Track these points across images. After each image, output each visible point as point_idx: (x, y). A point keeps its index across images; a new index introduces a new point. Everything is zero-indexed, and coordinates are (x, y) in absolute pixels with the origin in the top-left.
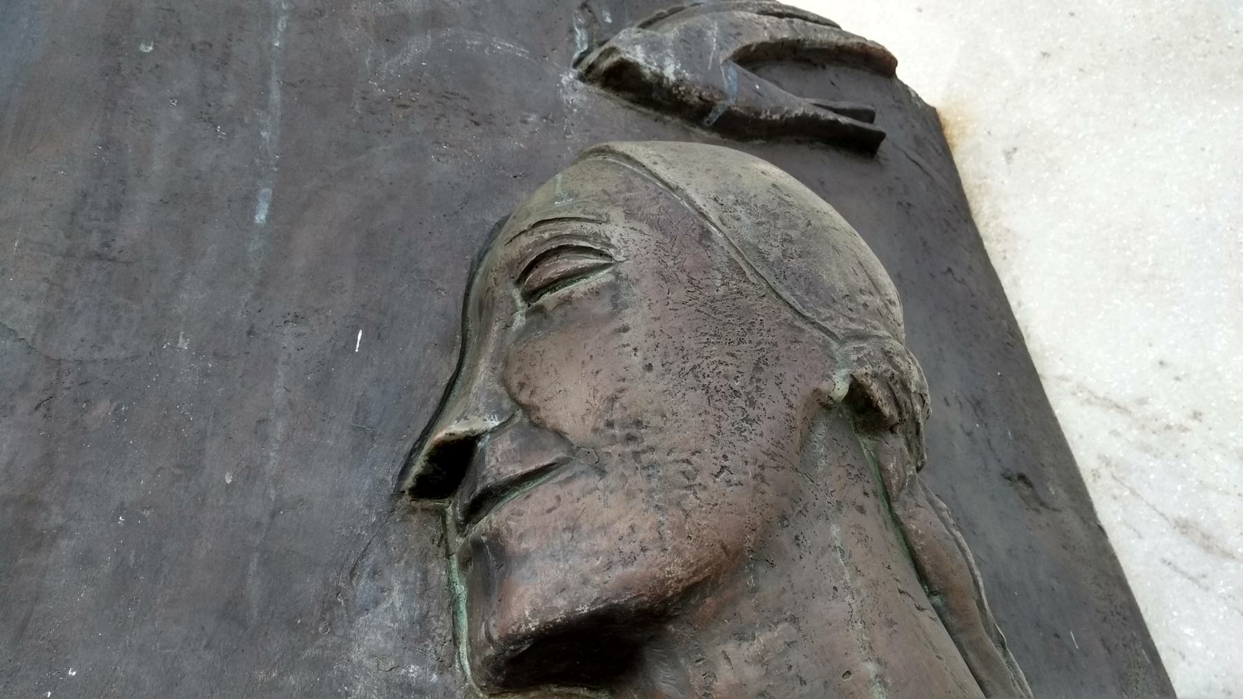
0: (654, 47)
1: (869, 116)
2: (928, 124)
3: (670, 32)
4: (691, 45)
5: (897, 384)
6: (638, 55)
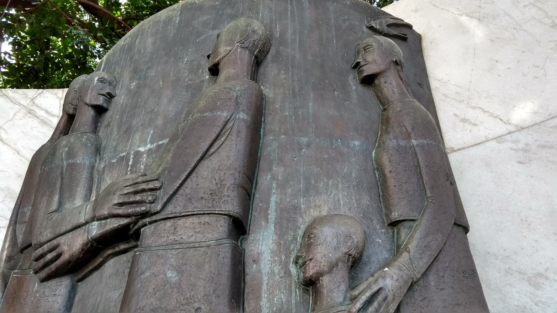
0: (376, 24)
1: (406, 35)
2: (419, 38)
3: (378, 22)
4: (381, 24)
5: (400, 61)
6: (374, 25)
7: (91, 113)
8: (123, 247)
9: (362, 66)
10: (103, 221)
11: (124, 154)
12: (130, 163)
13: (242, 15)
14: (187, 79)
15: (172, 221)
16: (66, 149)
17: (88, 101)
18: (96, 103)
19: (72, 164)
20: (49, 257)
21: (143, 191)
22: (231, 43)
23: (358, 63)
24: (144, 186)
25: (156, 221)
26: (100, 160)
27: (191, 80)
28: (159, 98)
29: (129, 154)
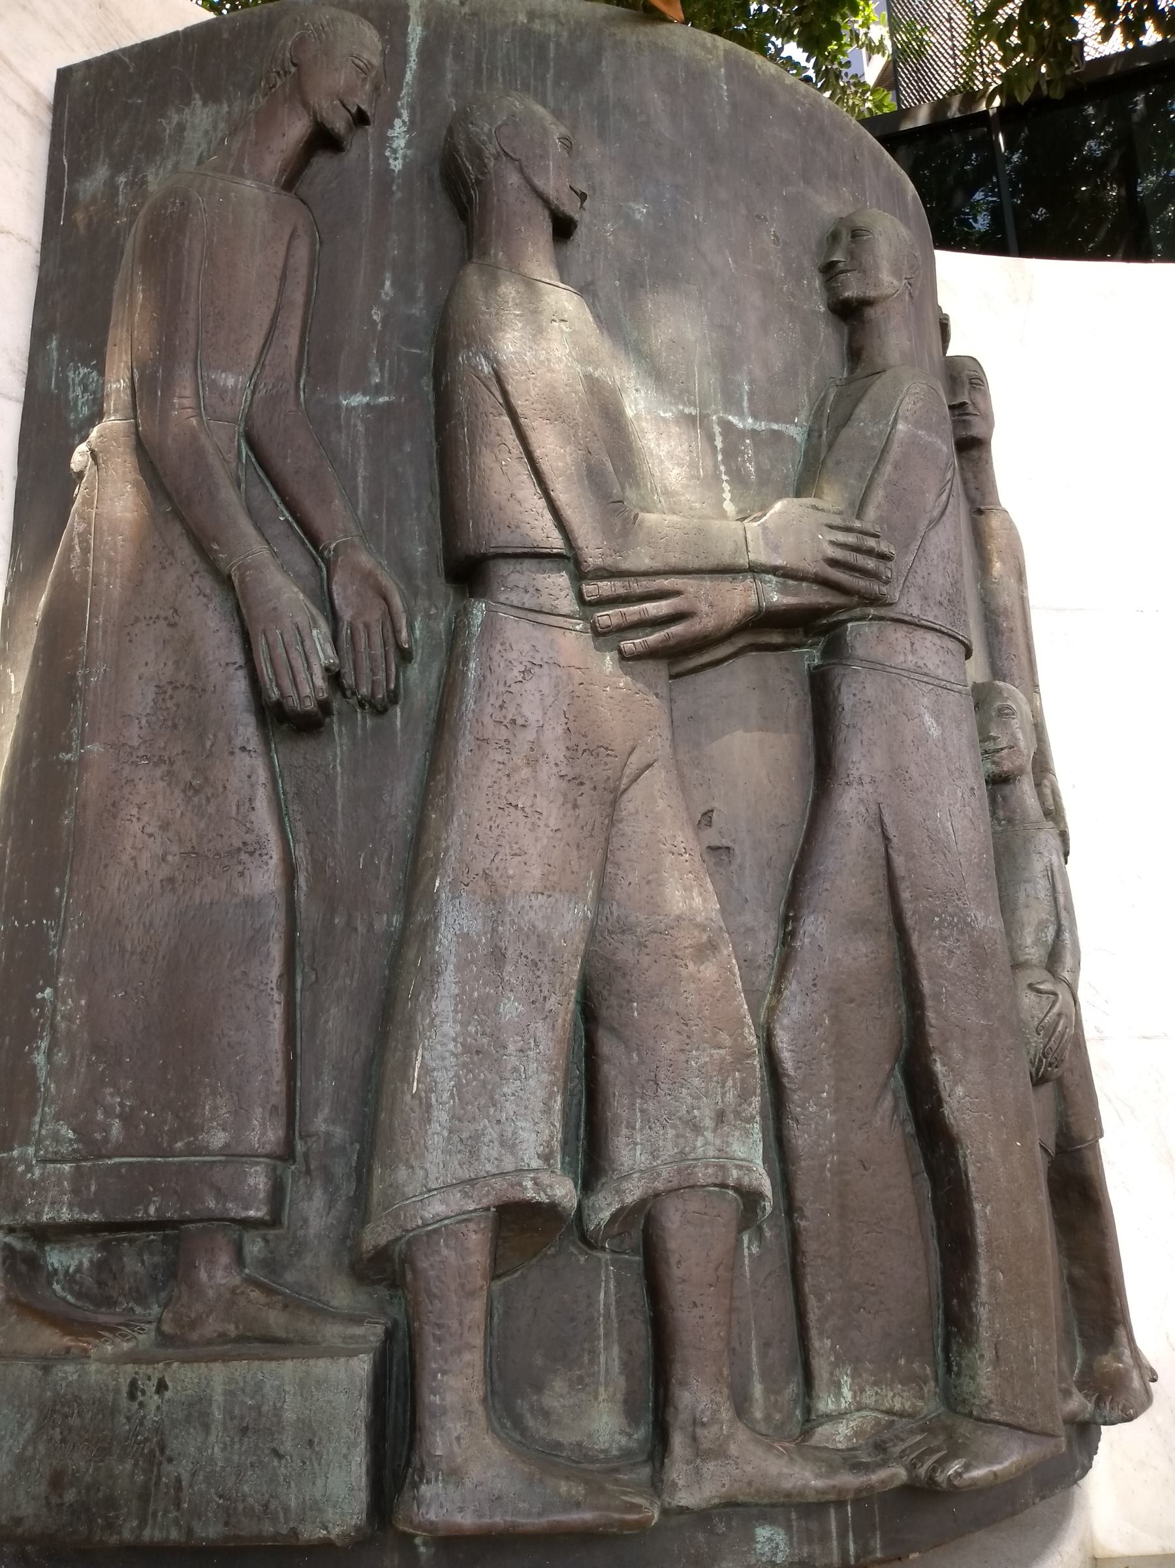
8: (777, 638)
9: (968, 414)
10: (791, 582)
12: (719, 443)
15: (905, 627)
17: (551, 193)
20: (654, 608)
21: (870, 552)
23: (963, 404)
24: (871, 543)
25: (881, 618)
27: (793, 295)
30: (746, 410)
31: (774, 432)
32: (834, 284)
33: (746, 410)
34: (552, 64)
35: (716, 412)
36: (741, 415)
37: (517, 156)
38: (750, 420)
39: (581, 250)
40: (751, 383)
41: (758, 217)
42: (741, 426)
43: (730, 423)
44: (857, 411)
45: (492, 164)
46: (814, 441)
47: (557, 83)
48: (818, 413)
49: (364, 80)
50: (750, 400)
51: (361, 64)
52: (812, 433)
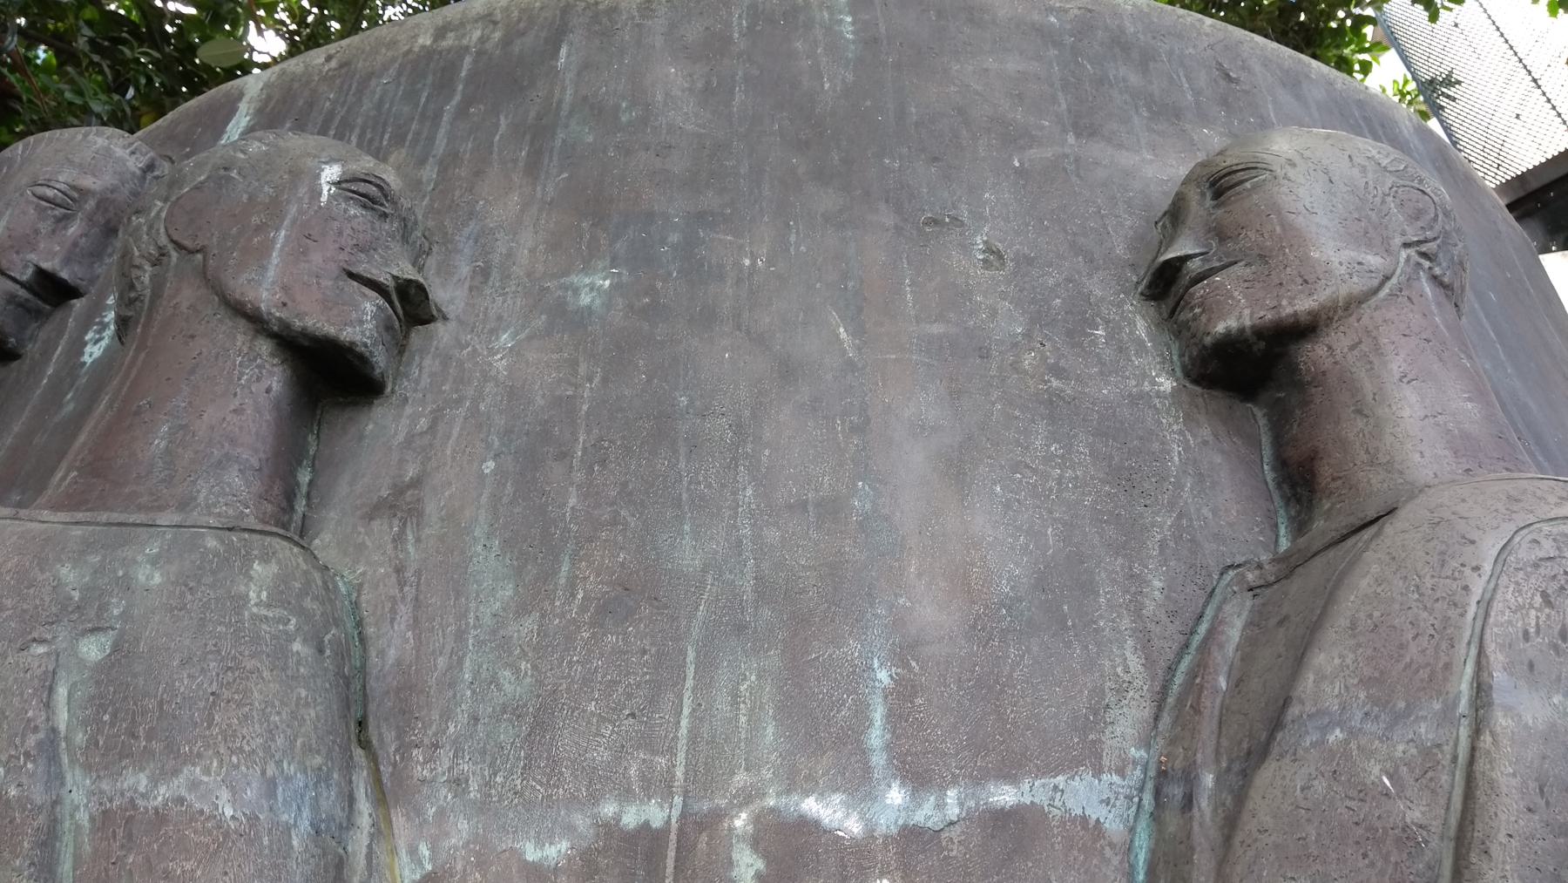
7: (265, 380)
11: (655, 814)
13: (1204, 119)
14: (1028, 360)
16: (93, 649)
17: (265, 294)
18: (330, 330)
19: (160, 817)
22: (1366, 231)
26: (381, 798)
27: (1058, 372)
28: (856, 429)
29: (701, 827)
30: (878, 760)
31: (1001, 819)
32: (1184, 316)
33: (878, 760)
34: (460, 87)
35: (747, 797)
36: (860, 786)
37: (200, 242)
38: (896, 795)
39: (408, 410)
40: (900, 656)
41: (934, 222)
42: (854, 827)
43: (808, 827)
44: (1308, 680)
45: (146, 279)
46: (1173, 823)
47: (462, 112)
48: (1176, 704)
49: (63, 221)
50: (893, 718)
51: (50, 193)
52: (1168, 788)
